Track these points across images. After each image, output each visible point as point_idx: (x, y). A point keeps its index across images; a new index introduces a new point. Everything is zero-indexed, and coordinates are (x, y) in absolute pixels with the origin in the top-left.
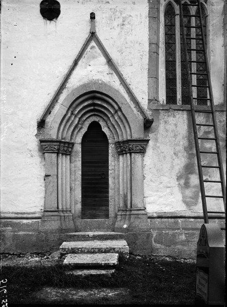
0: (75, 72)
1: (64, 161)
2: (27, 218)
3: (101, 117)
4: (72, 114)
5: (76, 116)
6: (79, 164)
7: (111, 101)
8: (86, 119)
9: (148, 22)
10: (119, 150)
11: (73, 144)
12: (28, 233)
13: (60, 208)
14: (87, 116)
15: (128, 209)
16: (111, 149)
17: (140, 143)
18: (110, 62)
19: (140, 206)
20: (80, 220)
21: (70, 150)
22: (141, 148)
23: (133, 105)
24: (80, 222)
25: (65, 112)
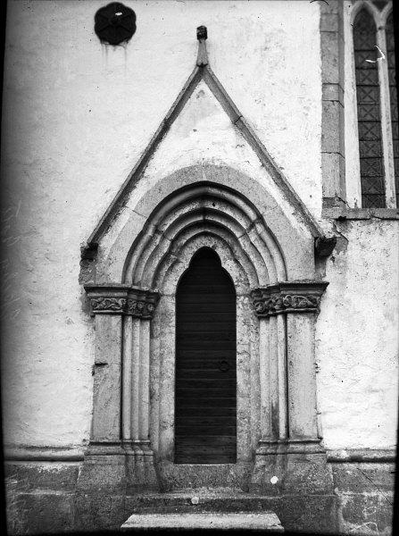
0: (163, 146)
1: (137, 334)
2: (53, 460)
3: (219, 238)
4: (157, 231)
5: (164, 237)
6: (170, 340)
7: (240, 203)
8: (188, 242)
9: (319, 41)
10: (259, 308)
11: (158, 296)
12: (53, 492)
13: (127, 436)
15: (283, 443)
16: (243, 309)
17: (305, 292)
18: (238, 121)
19: (309, 432)
20: (172, 466)
21: (151, 309)
22: (309, 303)
23: (288, 210)
24: (171, 469)
25: (140, 227)
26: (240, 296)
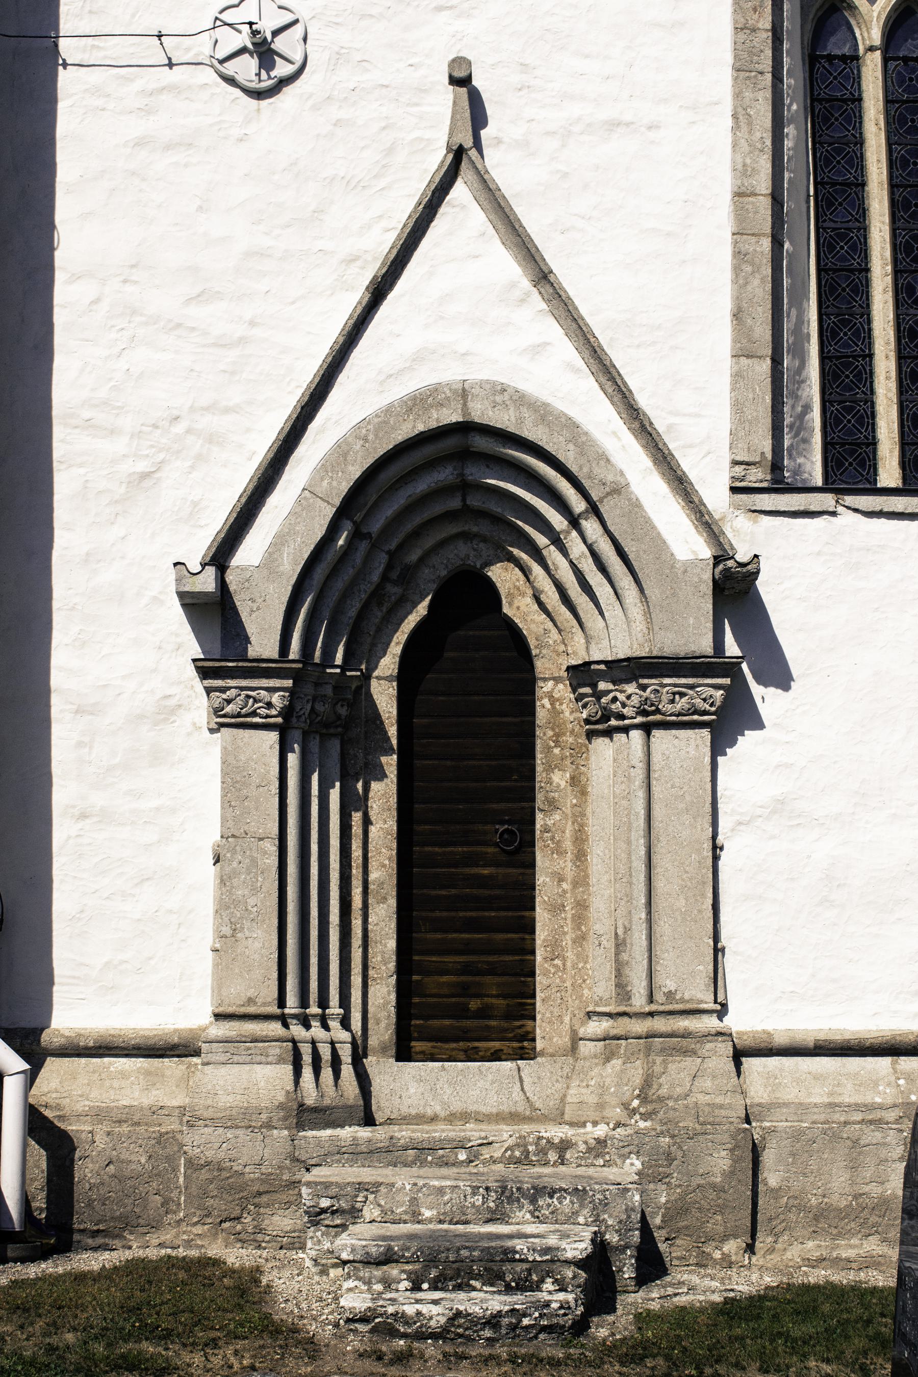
14: (429, 542)
17: (690, 681)
25: (319, 531)
26: (545, 680)
